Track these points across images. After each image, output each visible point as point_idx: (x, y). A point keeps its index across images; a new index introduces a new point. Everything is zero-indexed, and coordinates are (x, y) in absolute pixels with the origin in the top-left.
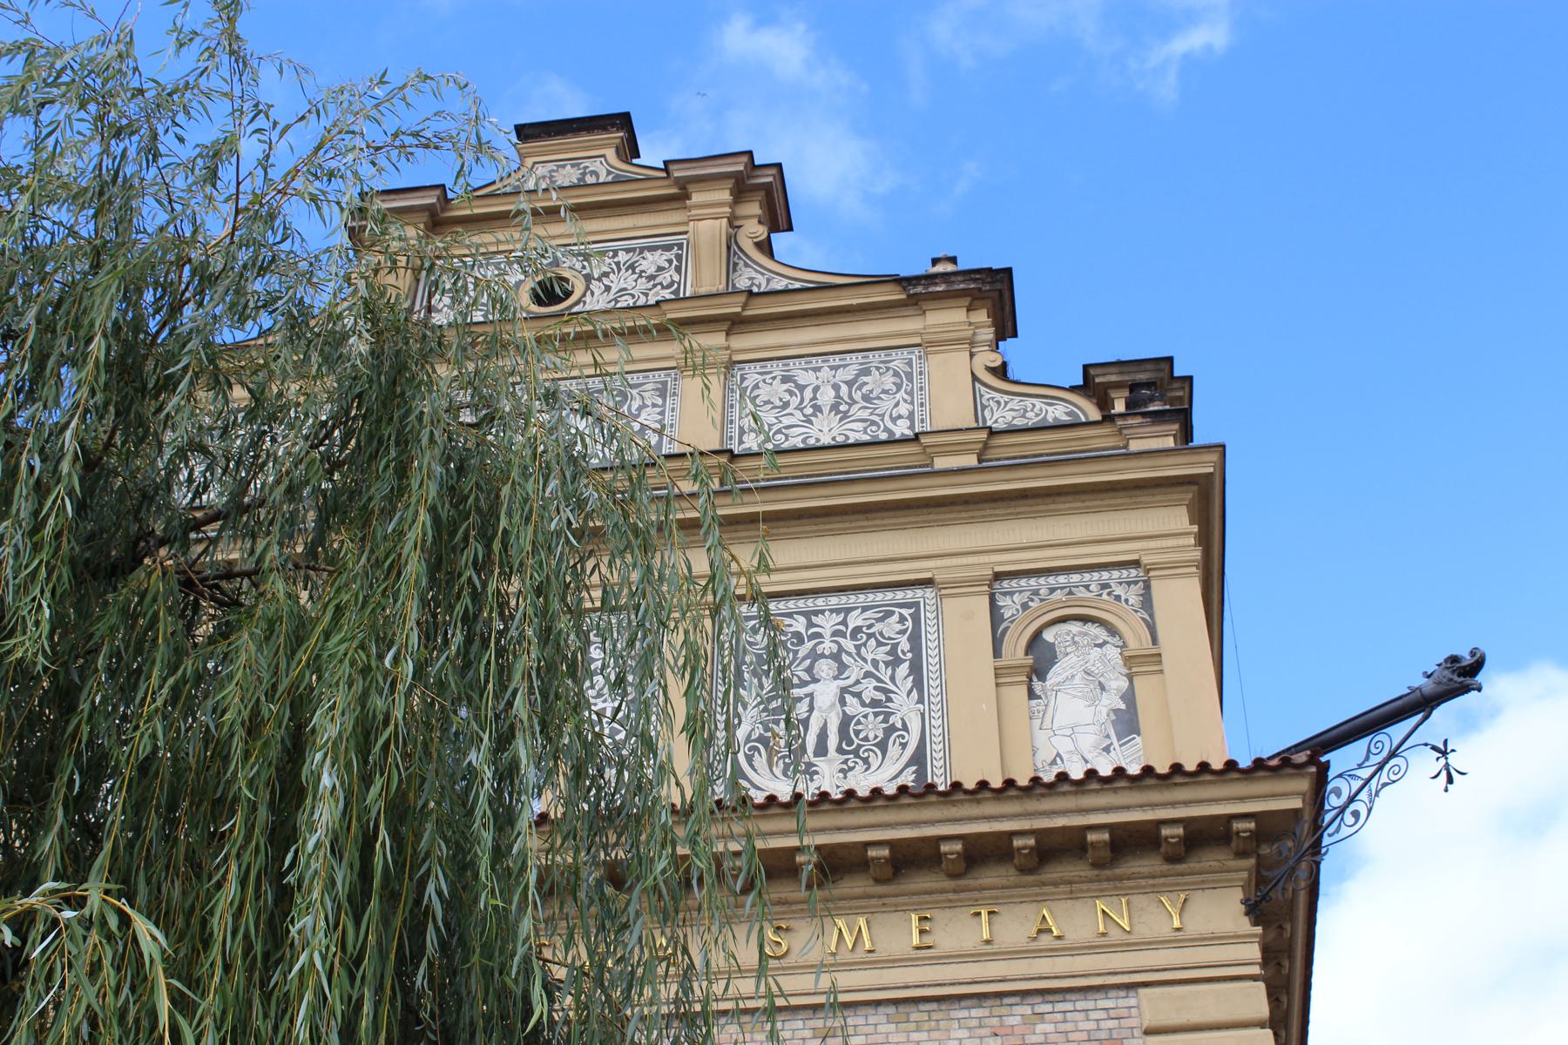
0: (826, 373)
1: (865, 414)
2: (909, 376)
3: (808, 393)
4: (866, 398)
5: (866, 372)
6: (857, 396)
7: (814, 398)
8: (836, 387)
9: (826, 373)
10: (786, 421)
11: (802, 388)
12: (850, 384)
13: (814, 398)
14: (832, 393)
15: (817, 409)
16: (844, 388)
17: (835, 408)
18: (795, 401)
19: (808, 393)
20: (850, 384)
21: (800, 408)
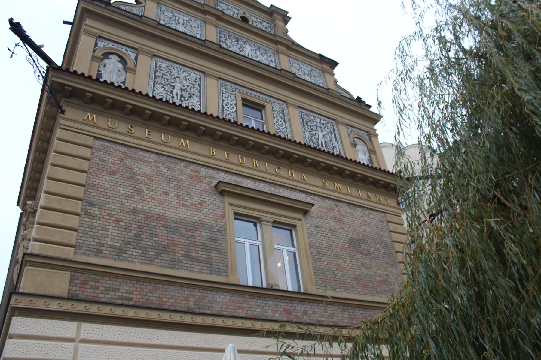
0: (181, 16)
1: (190, 29)
2: (201, 26)
3: (177, 18)
4: (191, 26)
5: (191, 20)
6: (189, 24)
7: (178, 20)
8: (184, 20)
9: (181, 16)
10: (171, 22)
11: (175, 17)
12: (187, 21)
13: (178, 20)
14: (182, 21)
15: (179, 23)
16: (185, 22)
17: (183, 24)
18: (173, 18)
19: (177, 18)
20: (187, 21)
21: (175, 20)
